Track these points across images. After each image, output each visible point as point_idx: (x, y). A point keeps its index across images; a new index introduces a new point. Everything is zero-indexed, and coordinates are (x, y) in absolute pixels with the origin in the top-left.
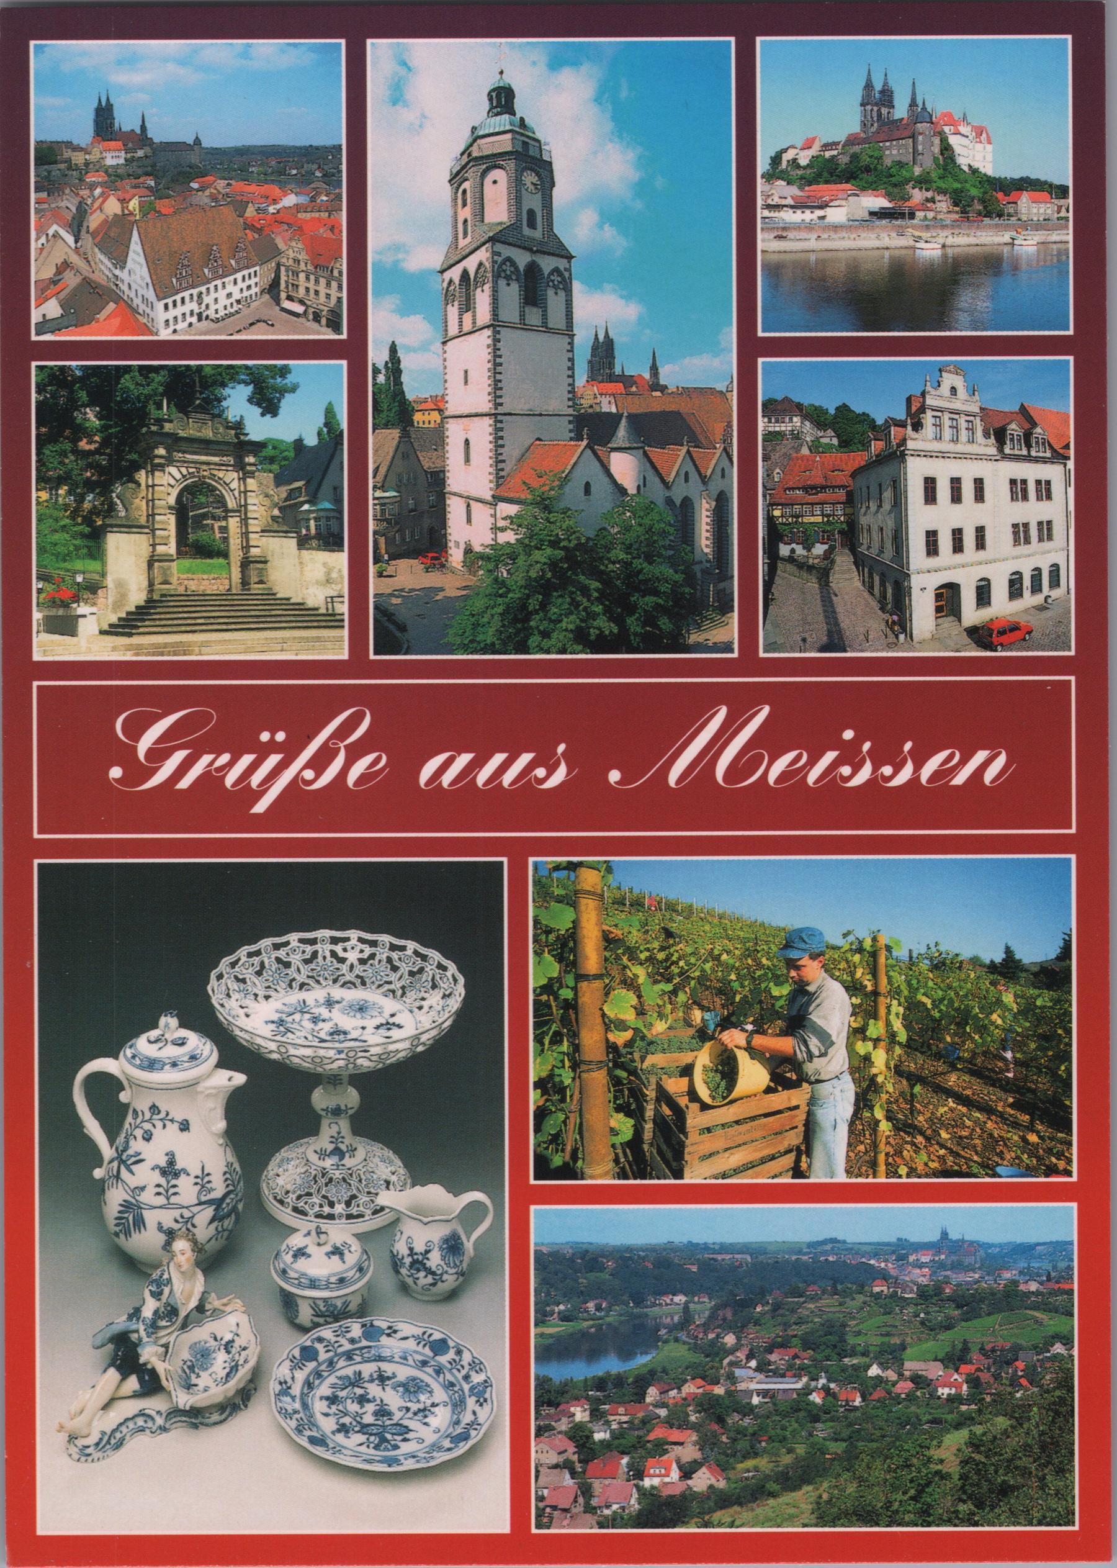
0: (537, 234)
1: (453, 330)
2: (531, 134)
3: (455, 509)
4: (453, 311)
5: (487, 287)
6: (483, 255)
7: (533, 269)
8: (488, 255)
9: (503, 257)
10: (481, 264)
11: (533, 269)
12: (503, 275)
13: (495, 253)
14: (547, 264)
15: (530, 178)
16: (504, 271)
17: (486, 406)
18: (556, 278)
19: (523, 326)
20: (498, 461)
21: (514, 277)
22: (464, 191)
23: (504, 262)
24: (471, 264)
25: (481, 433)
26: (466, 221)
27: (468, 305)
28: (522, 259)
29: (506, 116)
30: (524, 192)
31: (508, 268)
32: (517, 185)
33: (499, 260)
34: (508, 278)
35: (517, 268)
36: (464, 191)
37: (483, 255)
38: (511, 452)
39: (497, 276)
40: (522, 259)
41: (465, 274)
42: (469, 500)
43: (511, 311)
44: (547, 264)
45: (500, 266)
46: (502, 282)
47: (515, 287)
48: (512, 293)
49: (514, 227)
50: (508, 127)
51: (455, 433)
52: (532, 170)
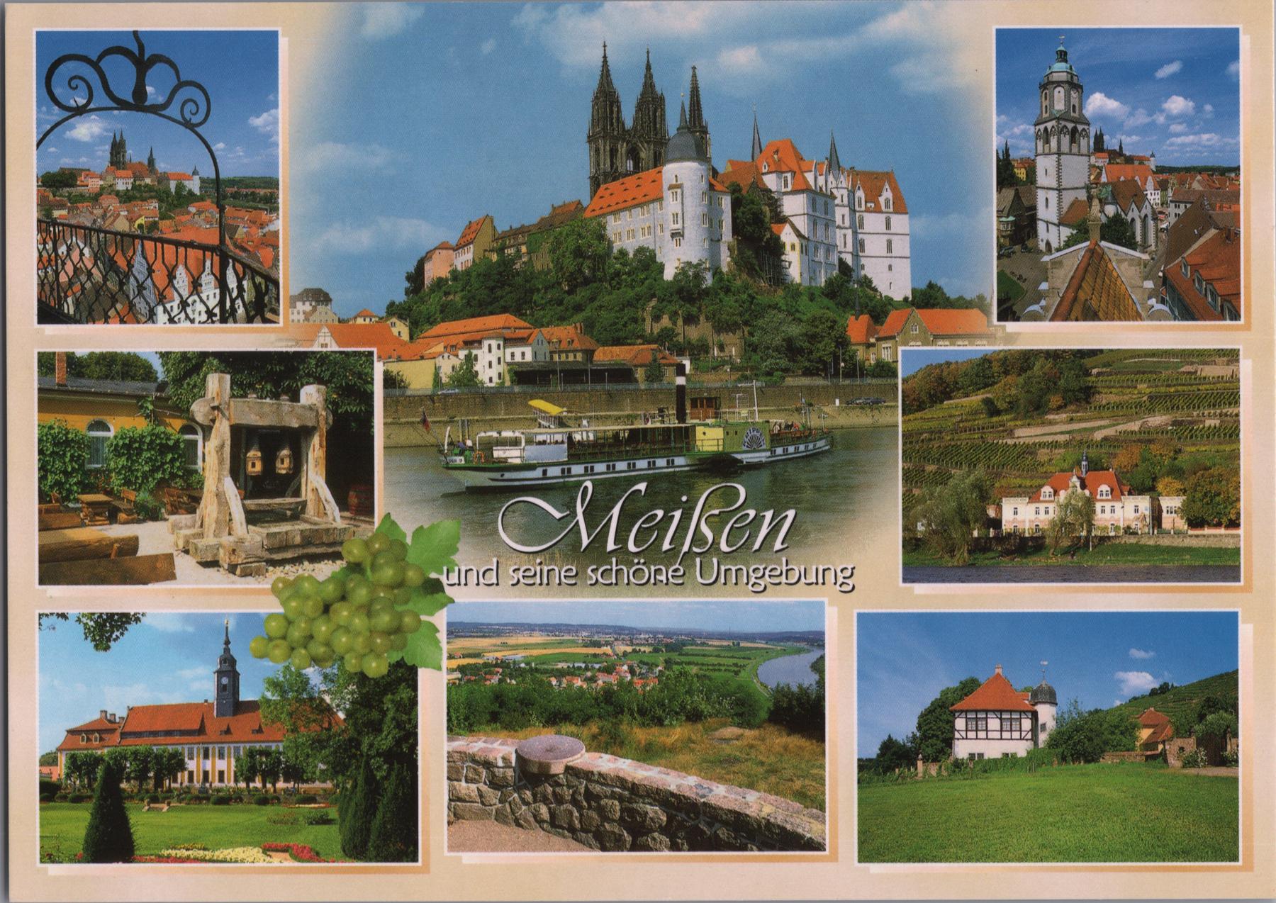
0: (1076, 115)
1: (1040, 150)
3: (1041, 227)
4: (1040, 144)
7: (1075, 129)
11: (1075, 129)
14: (1080, 127)
17: (1054, 185)
19: (1070, 153)
20: (1060, 208)
24: (1049, 125)
25: (1053, 196)
27: (1047, 141)
28: (1070, 126)
32: (1068, 98)
37: (1054, 123)
38: (1066, 205)
40: (1070, 126)
41: (1046, 129)
42: (1047, 222)
43: (1065, 148)
44: (1080, 127)
48: (1066, 140)
49: (1067, 112)
51: (1041, 195)
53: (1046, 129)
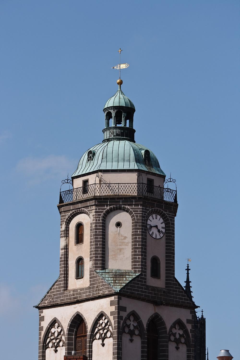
2: (154, 170)
5: (110, 342)
6: (106, 306)
7: (156, 322)
8: (113, 309)
9: (129, 311)
10: (101, 315)
11: (156, 322)
12: (127, 330)
13: (120, 309)
15: (156, 221)
16: (129, 326)
18: (178, 332)
21: (137, 332)
22: (80, 226)
23: (128, 318)
24: (89, 311)
26: (80, 261)
29: (124, 146)
30: (148, 237)
31: (132, 324)
32: (142, 230)
33: (124, 314)
34: (132, 333)
35: (140, 323)
36: (80, 226)
37: (106, 306)
39: (122, 330)
40: (146, 312)
41: (78, 321)
44: (170, 315)
45: (125, 322)
46: (126, 338)
47: (138, 341)
50: (134, 166)
52: (157, 213)
53: (78, 321)
